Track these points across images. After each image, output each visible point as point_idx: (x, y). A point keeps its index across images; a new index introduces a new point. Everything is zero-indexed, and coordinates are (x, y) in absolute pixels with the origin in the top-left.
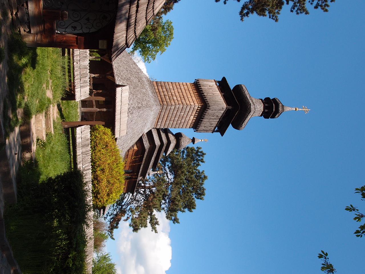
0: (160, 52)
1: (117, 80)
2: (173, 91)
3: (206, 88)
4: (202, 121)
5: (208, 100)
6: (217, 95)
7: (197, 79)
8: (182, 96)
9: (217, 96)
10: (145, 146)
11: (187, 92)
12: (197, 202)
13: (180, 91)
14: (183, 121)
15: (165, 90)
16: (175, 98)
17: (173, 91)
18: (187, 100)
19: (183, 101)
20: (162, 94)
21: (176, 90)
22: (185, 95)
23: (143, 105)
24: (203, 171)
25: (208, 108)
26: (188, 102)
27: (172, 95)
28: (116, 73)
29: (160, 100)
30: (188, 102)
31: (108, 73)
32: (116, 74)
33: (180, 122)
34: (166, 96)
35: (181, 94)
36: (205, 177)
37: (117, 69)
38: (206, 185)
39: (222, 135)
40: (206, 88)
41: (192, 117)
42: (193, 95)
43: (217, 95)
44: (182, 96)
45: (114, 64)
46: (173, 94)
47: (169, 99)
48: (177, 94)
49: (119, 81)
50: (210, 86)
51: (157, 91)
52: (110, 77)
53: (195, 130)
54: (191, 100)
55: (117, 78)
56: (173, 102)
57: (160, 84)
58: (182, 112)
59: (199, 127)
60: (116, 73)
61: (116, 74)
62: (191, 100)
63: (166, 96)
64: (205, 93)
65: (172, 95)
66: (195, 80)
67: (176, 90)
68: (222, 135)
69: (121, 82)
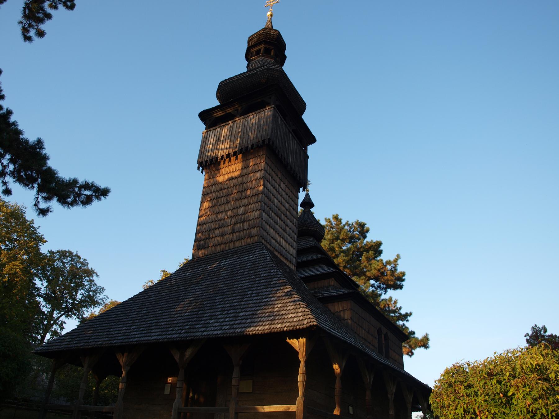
0: (95, 278)
1: (205, 333)
4: (291, 168)
7: (197, 165)
10: (342, 292)
12: (371, 238)
14: (287, 205)
15: (217, 232)
16: (241, 210)
20: (228, 237)
23: (272, 274)
24: (326, 219)
25: (273, 143)
28: (180, 333)
31: (177, 357)
32: (186, 335)
33: (288, 213)
36: (336, 218)
37: (168, 331)
38: (349, 217)
39: (312, 140)
41: (283, 185)
45: (154, 338)
47: (244, 222)
49: (210, 329)
52: (189, 353)
53: (301, 189)
55: (200, 334)
56: (252, 215)
58: (274, 200)
59: (300, 177)
60: (180, 333)
61: (186, 335)
66: (199, 169)
68: (312, 140)
69: (208, 323)
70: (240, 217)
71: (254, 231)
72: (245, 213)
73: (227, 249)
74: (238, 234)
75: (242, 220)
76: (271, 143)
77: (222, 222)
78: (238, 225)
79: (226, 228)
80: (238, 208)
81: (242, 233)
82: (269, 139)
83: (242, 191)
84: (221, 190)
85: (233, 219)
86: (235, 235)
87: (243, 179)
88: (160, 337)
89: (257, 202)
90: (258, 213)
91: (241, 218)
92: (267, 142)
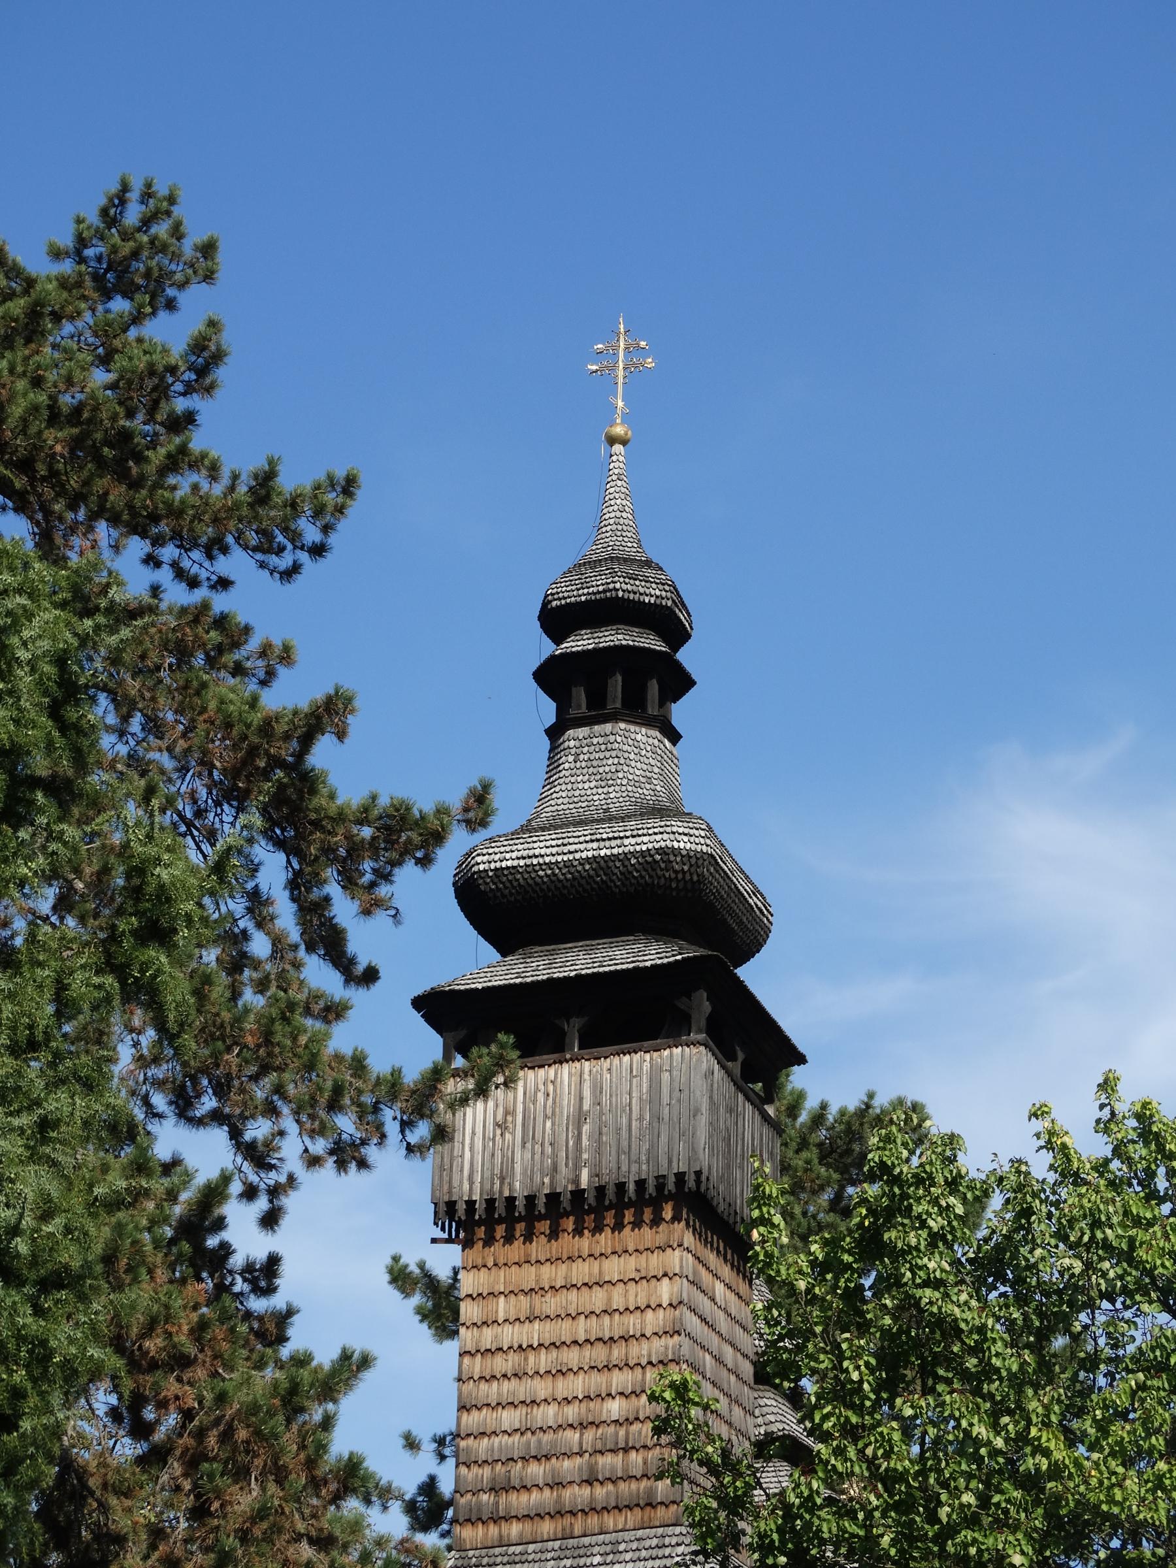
2: (552, 1410)
3: (521, 1159)
5: (645, 1170)
6: (587, 1093)
9: (597, 1089)
11: (551, 1304)
13: (544, 1360)
15: (536, 1471)
17: (548, 1414)
18: (632, 1323)
20: (580, 1495)
21: (541, 1388)
22: (581, 1329)
26: (653, 1321)
27: (583, 1426)
30: (653, 1321)
34: (592, 1469)
35: (572, 1357)
40: (521, 1159)
42: (581, 1271)
43: (587, 1093)
44: (599, 1354)
46: (571, 1412)
47: (626, 1450)
48: (577, 1385)
50: (502, 1126)
51: (547, 1527)
54: (638, 1294)
57: (485, 1497)
62: (638, 1294)
63: (592, 1469)
64: (576, 1180)
65: (583, 1426)
67: (541, 1388)
70: (612, 1429)
73: (577, 1532)
74: (610, 1487)
75: (622, 1444)
76: (703, 1189)
77: (547, 1438)
79: (567, 1463)
81: (622, 1486)
82: (698, 1174)
83: (611, 1338)
84: (530, 1319)
85: (590, 1435)
86: (600, 1492)
91: (617, 1434)
92: (691, 1184)
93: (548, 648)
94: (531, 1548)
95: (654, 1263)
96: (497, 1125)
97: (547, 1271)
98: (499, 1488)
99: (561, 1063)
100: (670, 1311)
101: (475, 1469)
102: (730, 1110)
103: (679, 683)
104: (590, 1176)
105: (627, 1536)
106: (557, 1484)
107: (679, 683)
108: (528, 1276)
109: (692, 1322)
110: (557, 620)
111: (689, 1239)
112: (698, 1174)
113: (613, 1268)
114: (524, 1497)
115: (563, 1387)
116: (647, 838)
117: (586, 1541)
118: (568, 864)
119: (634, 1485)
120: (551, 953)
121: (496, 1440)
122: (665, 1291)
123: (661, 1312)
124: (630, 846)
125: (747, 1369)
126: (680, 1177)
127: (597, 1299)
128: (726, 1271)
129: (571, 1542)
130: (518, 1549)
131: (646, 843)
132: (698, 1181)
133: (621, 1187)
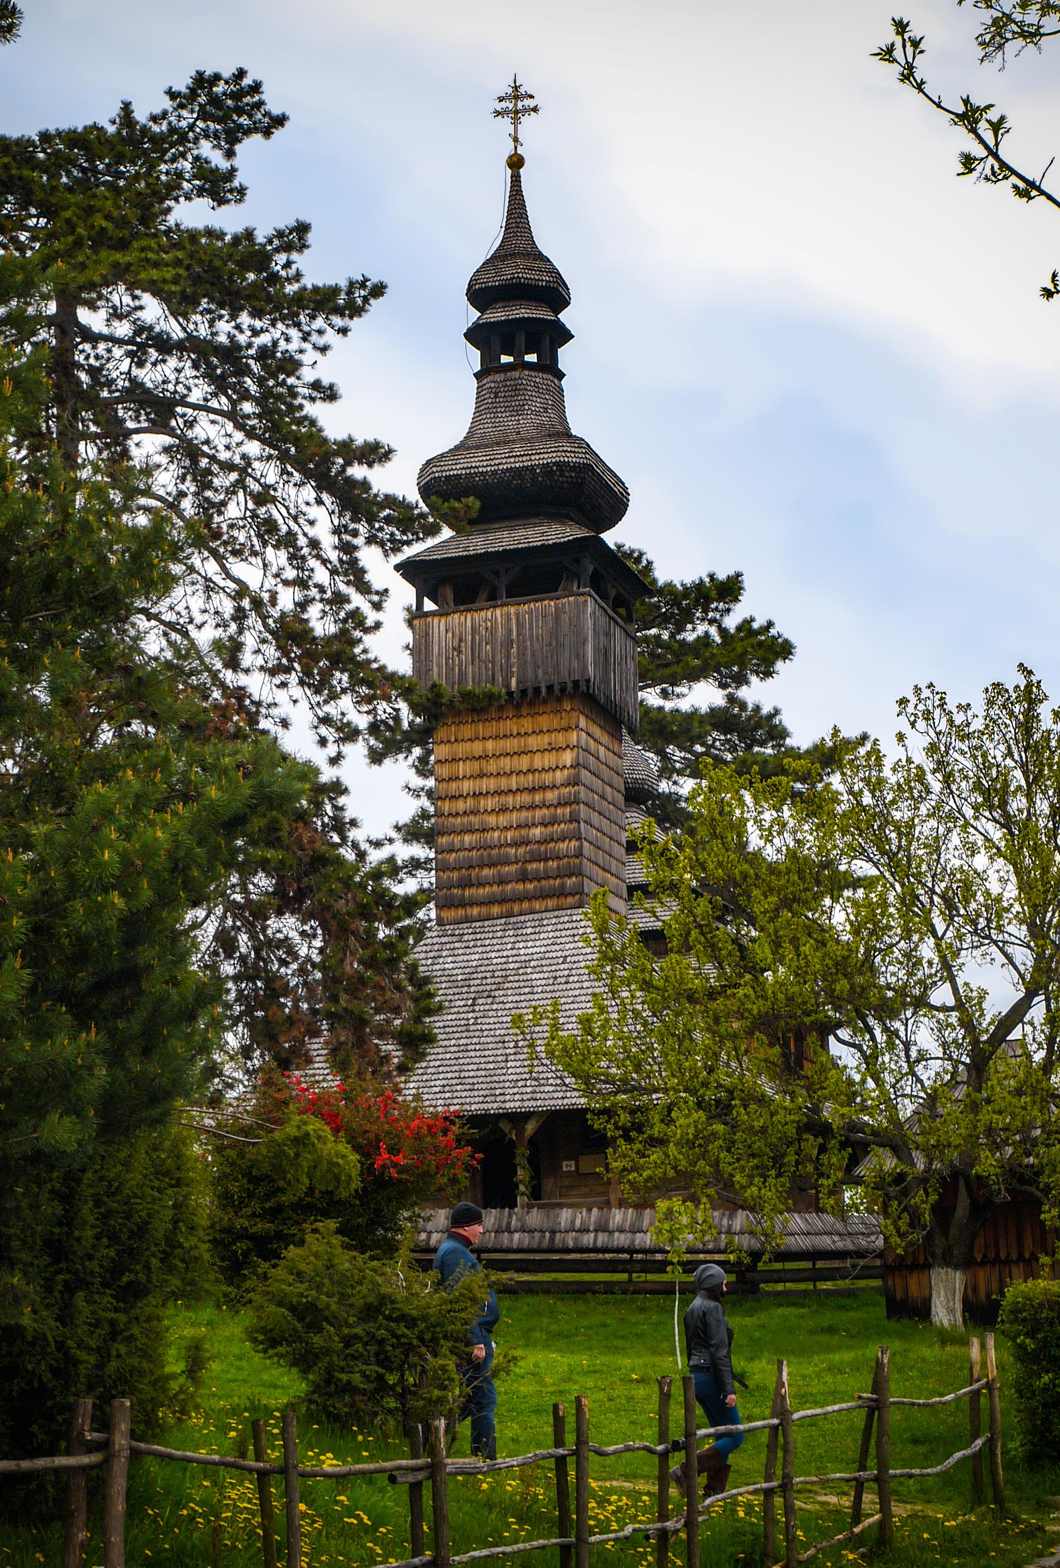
8: (526, 798)
11: (492, 767)
13: (490, 803)
16: (537, 832)
18: (547, 778)
19: (551, 796)
22: (514, 782)
26: (559, 776)
27: (516, 844)
29: (551, 903)
30: (559, 776)
44: (526, 798)
47: (546, 860)
52: (531, 1127)
54: (549, 760)
62: (549, 760)
64: (508, 686)
67: (492, 820)
71: (570, 882)
72: (546, 842)
74: (536, 883)
77: (495, 852)
78: (535, 865)
80: (527, 826)
81: (543, 882)
85: (521, 850)
86: (530, 886)
87: (532, 762)
88: (490, 1106)
89: (571, 821)
90: (574, 844)
92: (583, 687)
93: (475, 314)
94: (486, 923)
95: (560, 739)
96: (454, 649)
97: (490, 745)
98: (465, 883)
99: (495, 607)
100: (572, 771)
101: (448, 873)
102: (607, 634)
103: (564, 336)
104: (518, 682)
105: (548, 915)
106: (502, 881)
107: (564, 336)
108: (477, 748)
109: (585, 774)
110: (480, 295)
111: (583, 722)
112: (588, 681)
113: (533, 742)
114: (481, 891)
115: (503, 820)
116: (547, 455)
117: (522, 918)
118: (494, 473)
119: (552, 882)
120: (485, 532)
121: (461, 854)
122: (568, 757)
123: (566, 772)
124: (537, 460)
125: (620, 799)
126: (576, 683)
127: (524, 762)
128: (605, 738)
129: (513, 920)
130: (478, 924)
131: (547, 458)
132: (588, 687)
133: (537, 690)
